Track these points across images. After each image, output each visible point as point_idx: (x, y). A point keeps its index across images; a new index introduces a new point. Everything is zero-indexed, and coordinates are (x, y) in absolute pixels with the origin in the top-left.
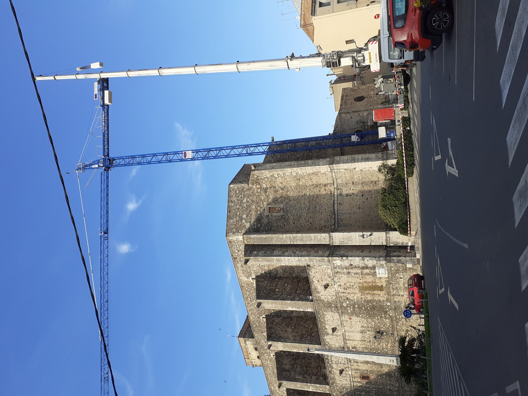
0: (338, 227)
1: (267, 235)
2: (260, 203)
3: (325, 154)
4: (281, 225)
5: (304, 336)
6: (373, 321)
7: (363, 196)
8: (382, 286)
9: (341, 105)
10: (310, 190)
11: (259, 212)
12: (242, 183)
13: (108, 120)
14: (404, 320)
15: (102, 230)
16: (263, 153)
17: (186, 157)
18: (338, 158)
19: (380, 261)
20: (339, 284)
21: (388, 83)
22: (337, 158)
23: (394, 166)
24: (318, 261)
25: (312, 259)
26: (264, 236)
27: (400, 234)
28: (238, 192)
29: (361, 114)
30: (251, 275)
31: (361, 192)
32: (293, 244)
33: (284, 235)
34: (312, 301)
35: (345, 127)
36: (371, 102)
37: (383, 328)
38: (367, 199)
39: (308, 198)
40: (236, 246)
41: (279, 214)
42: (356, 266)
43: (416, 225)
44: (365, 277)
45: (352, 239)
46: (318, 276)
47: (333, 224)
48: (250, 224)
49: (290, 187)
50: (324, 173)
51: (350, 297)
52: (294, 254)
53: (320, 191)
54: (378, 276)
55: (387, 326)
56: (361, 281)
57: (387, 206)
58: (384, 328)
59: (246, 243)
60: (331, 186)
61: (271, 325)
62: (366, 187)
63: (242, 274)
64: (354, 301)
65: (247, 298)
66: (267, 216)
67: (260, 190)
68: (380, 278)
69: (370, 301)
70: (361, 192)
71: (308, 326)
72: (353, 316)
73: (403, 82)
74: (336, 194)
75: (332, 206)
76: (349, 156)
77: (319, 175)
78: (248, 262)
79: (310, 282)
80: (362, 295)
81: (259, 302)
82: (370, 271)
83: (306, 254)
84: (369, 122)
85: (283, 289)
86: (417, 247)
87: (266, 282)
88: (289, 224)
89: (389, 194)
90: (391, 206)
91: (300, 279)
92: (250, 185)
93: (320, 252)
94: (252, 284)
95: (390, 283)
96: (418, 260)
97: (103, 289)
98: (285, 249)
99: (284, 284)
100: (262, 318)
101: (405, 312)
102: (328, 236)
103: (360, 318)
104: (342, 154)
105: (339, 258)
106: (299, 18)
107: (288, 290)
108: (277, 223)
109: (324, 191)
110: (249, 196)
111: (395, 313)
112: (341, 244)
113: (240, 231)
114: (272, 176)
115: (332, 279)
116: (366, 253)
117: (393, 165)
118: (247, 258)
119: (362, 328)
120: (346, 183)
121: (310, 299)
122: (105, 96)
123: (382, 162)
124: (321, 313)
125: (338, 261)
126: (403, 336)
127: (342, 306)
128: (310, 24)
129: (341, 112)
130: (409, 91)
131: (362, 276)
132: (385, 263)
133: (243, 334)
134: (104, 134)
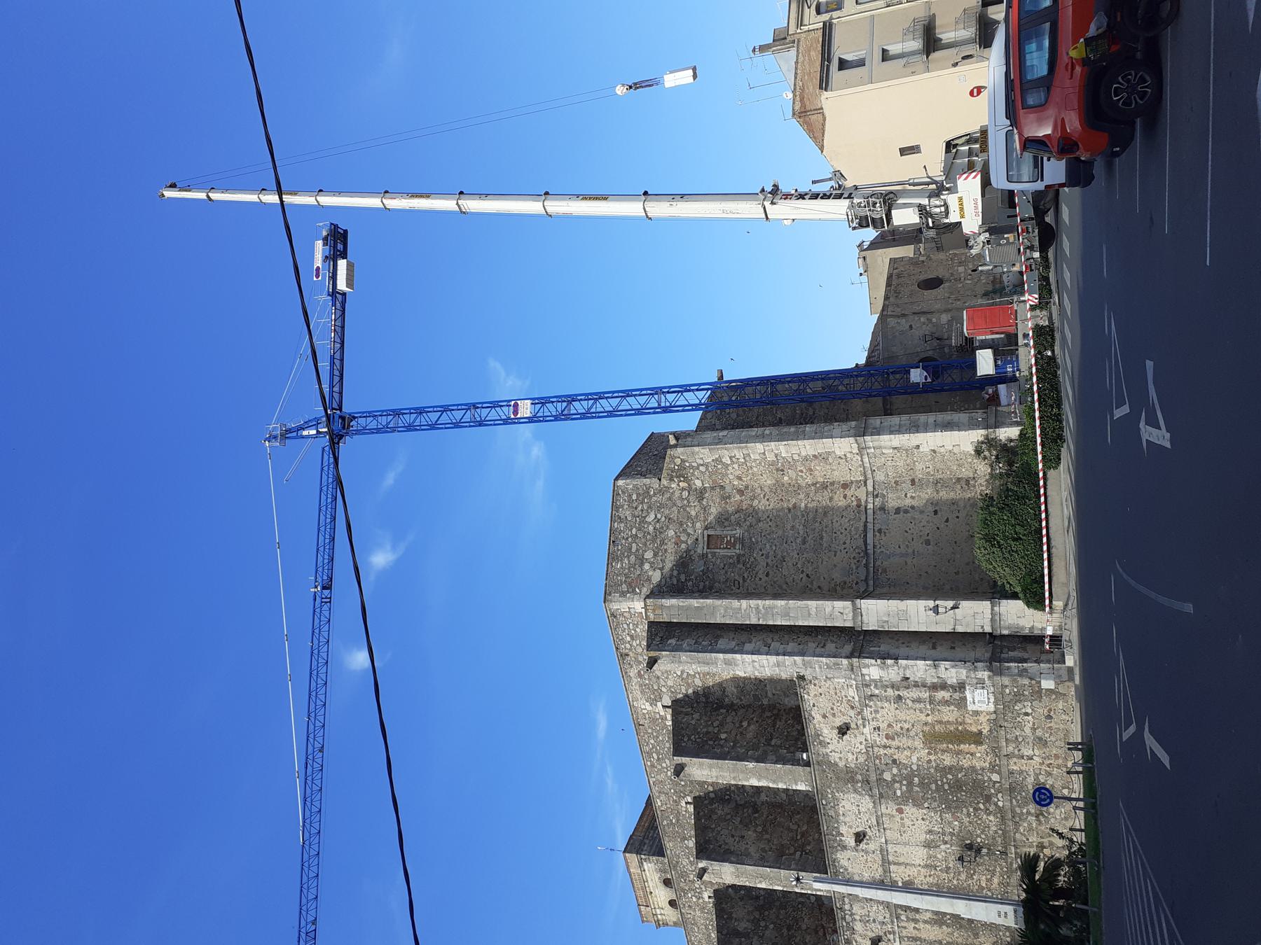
0: (875, 586)
1: (702, 600)
2: (687, 525)
3: (844, 411)
4: (737, 578)
5: (787, 852)
6: (956, 819)
7: (936, 512)
8: (980, 733)
9: (886, 298)
10: (808, 495)
11: (683, 546)
12: (645, 476)
13: (343, 327)
14: (1034, 818)
15: (319, 579)
16: (695, 407)
17: (518, 414)
18: (878, 422)
19: (977, 671)
20: (875, 724)
21: (1000, 245)
22: (876, 421)
23: (1012, 444)
24: (825, 667)
25: (809, 662)
26: (695, 603)
27: (1026, 607)
28: (634, 497)
29: (934, 320)
30: (661, 698)
31: (932, 503)
32: (764, 623)
33: (744, 603)
34: (807, 764)
35: (894, 349)
36: (959, 292)
37: (981, 838)
38: (947, 521)
39: (803, 516)
40: (628, 625)
42: (917, 682)
43: (1067, 585)
44: (939, 710)
45: (910, 617)
46: (824, 703)
47: (864, 578)
48: (662, 575)
49: (759, 489)
50: (843, 457)
51: (902, 757)
52: (767, 648)
53: (831, 499)
54: (971, 707)
55: (991, 832)
56: (929, 719)
57: (994, 539)
58: (983, 836)
59: (652, 617)
60: (859, 488)
61: (705, 820)
62: (945, 493)
63: (639, 695)
64: (911, 768)
65: (650, 754)
66: (704, 556)
67: (687, 494)
68: (976, 713)
69: (950, 768)
70: (932, 503)
71: (795, 827)
72: (907, 805)
73: (1036, 243)
74: (870, 506)
75: (860, 535)
76: (905, 417)
77: (830, 460)
78: (656, 665)
79: (805, 718)
80: (929, 754)
81: (680, 762)
82: (951, 696)
83: (796, 650)
84: (953, 338)
85: (736, 735)
86: (1068, 639)
87: (696, 716)
88: (755, 577)
89: (1001, 509)
90: (1005, 538)
91: (779, 710)
92: (664, 482)
93: (831, 647)
94: (663, 718)
95: (1001, 727)
96: (1070, 670)
97: (312, 719)
98: (744, 636)
99: (741, 722)
100: (683, 804)
101: (1037, 793)
102: (851, 606)
103: (925, 811)
104: (888, 412)
105: (876, 661)
106: (791, 95)
107: (750, 735)
108: (726, 572)
109: (842, 498)
110: (661, 506)
111: (1011, 801)
112: (883, 627)
113: (637, 590)
114: (717, 460)
115: (859, 713)
116: (942, 650)
117: (1011, 441)
118: (653, 654)
119: (928, 836)
120: (896, 482)
121: (803, 759)
122: (339, 272)
123: (983, 432)
124: (830, 796)
125: (873, 670)
126: (1032, 854)
127: (880, 780)
128: (814, 110)
129: (885, 313)
130: (1053, 266)
131: (932, 706)
132: (989, 677)
133: (637, 844)
134: (332, 358)
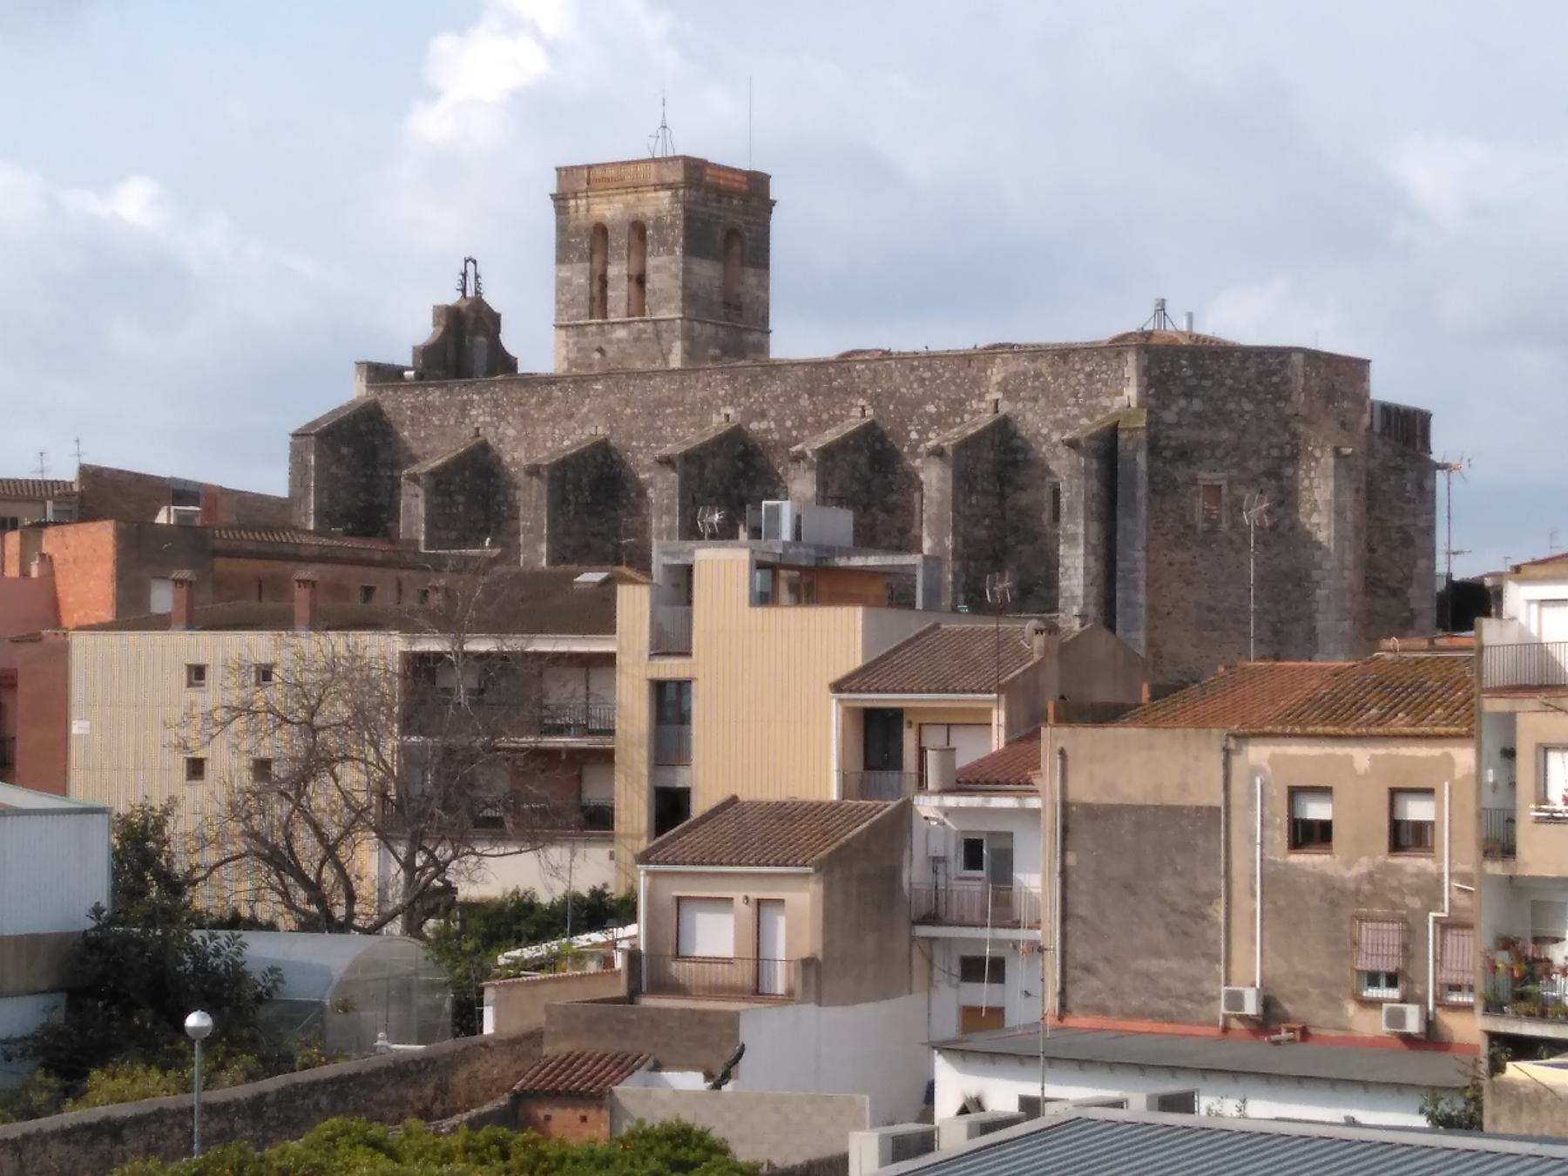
4: (1168, 525)
41: (1199, 516)
66: (1194, 481)
114: (1316, 506)
